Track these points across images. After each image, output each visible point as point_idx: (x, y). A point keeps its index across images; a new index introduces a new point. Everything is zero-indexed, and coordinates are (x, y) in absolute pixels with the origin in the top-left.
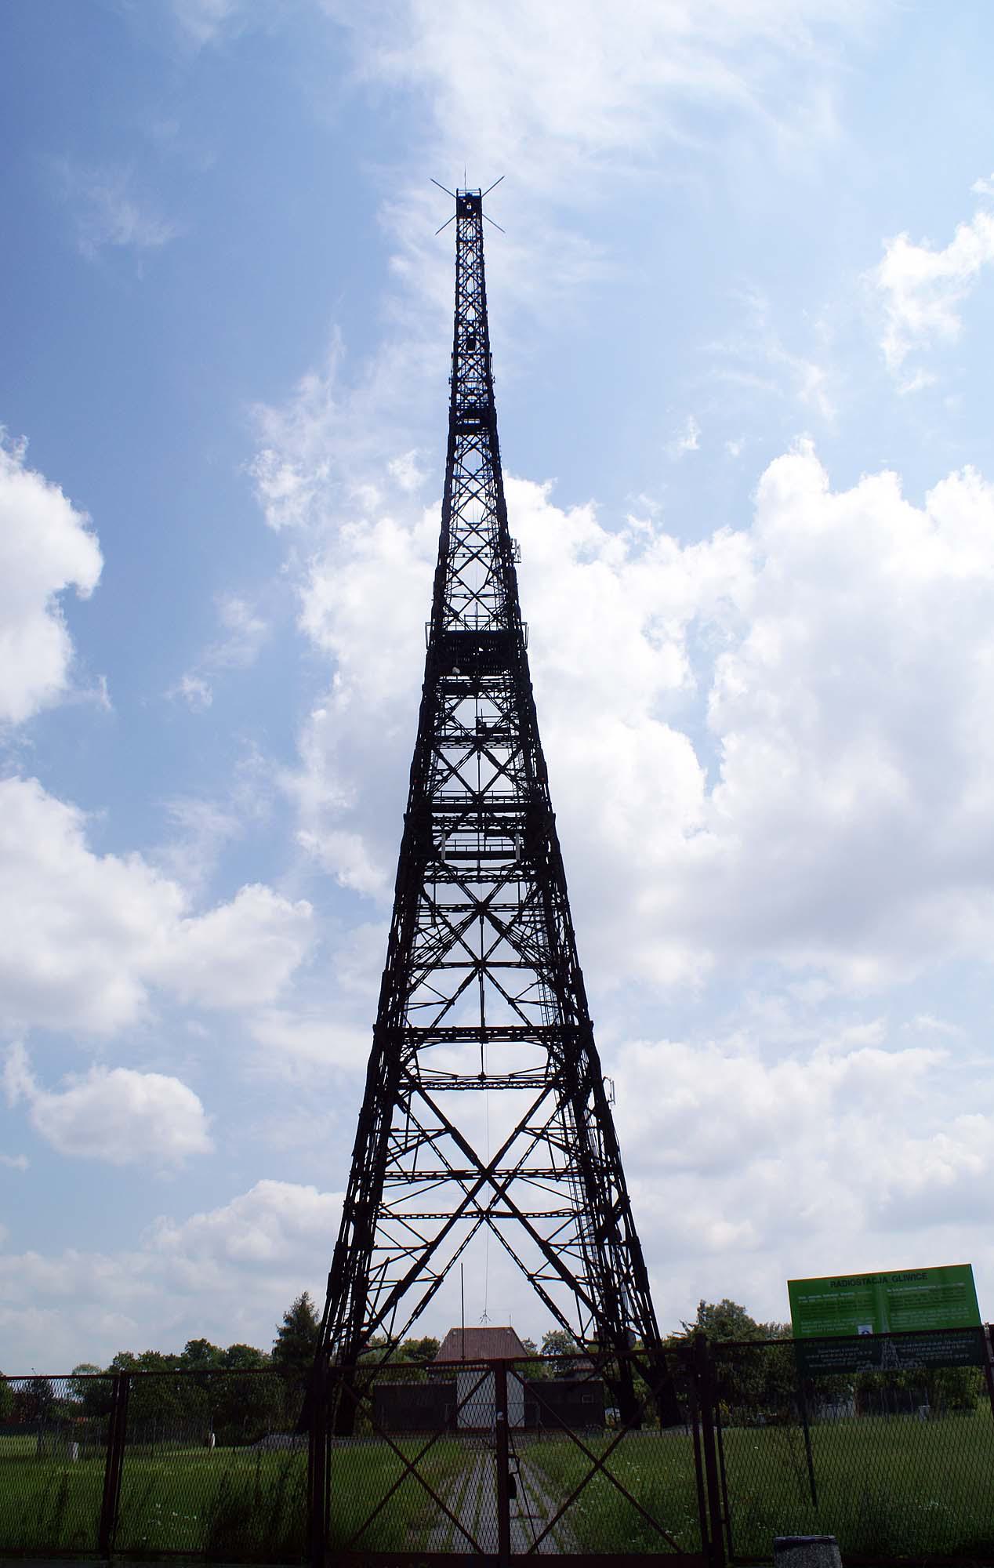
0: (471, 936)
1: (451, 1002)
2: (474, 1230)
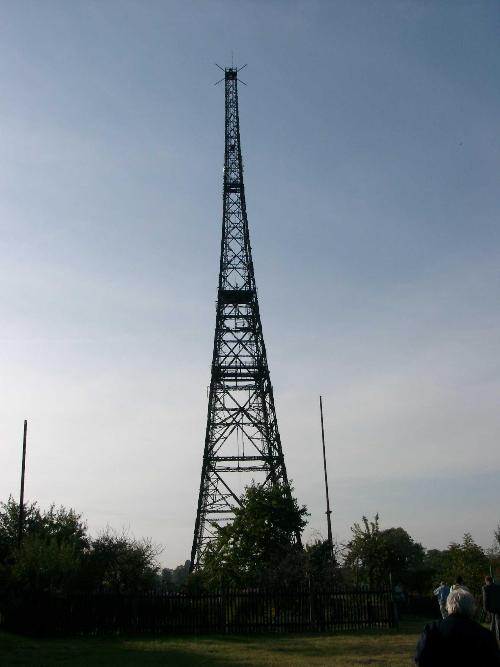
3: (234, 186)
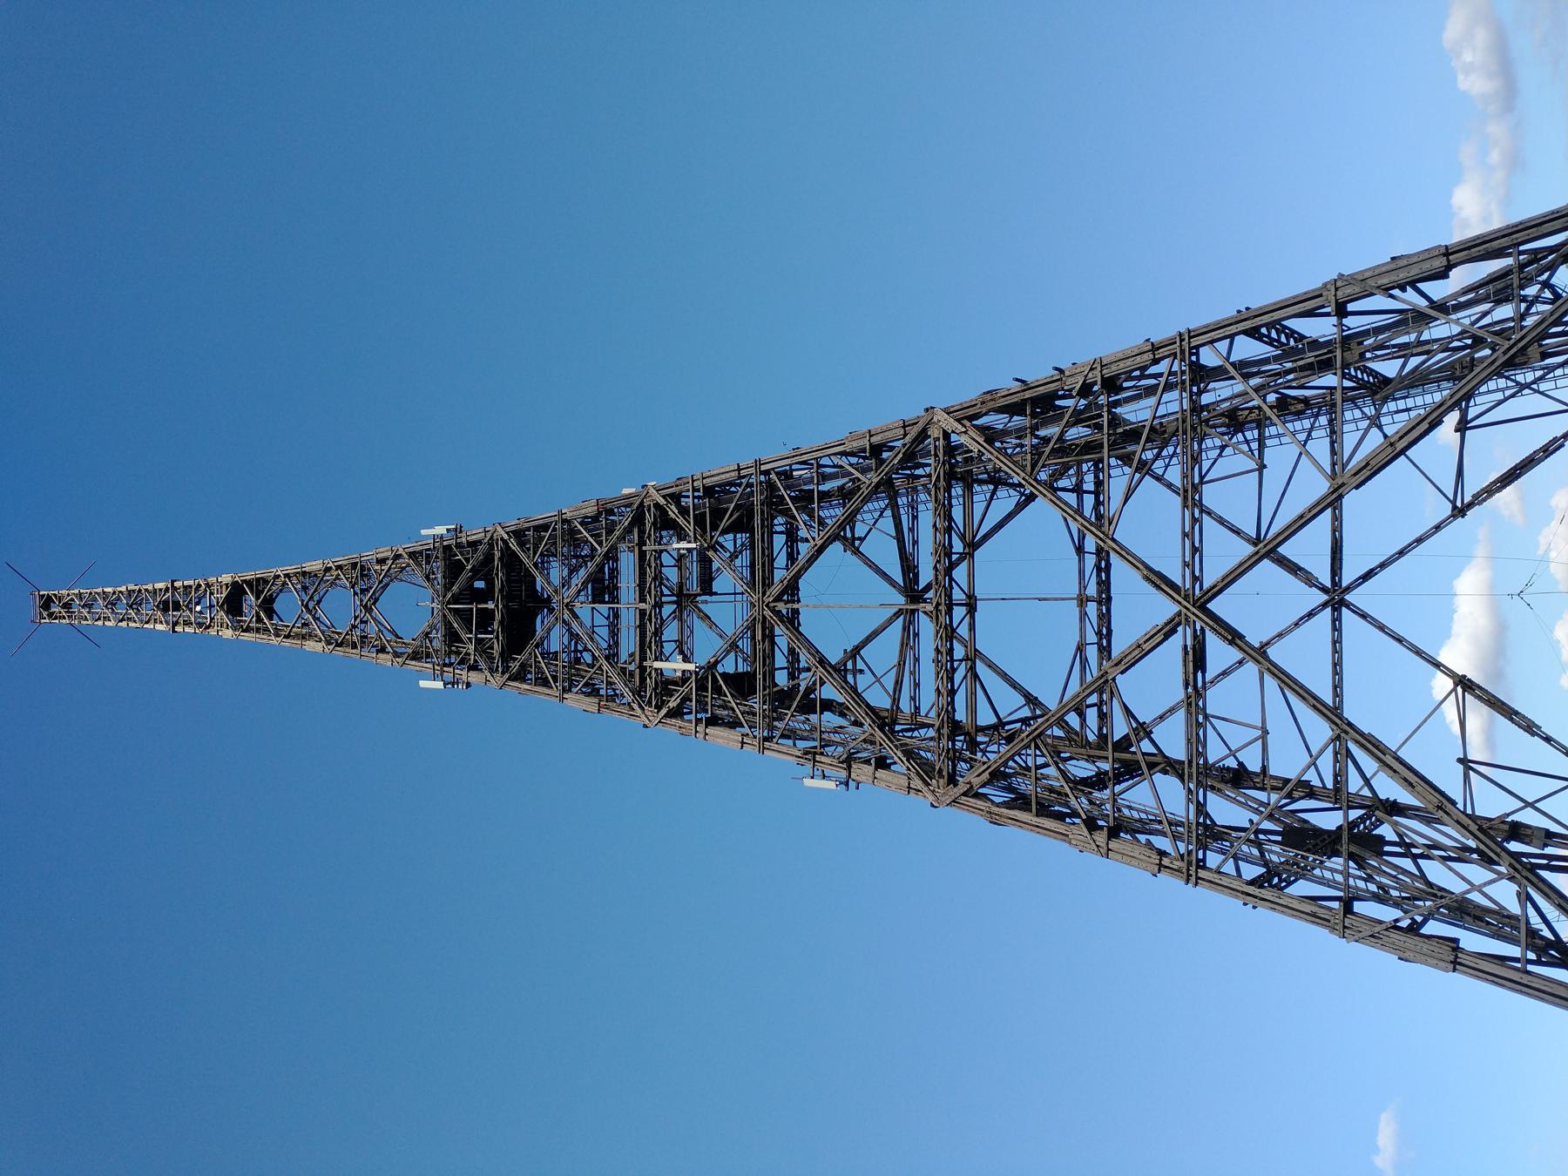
2: (1364, 616)
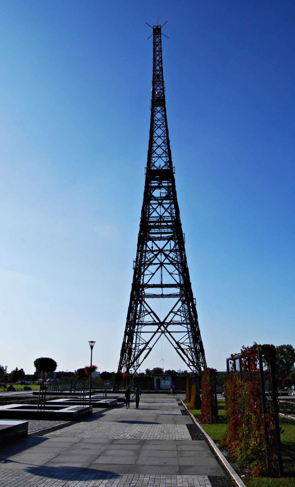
0: (159, 256)
1: (154, 274)
3: (158, 102)
